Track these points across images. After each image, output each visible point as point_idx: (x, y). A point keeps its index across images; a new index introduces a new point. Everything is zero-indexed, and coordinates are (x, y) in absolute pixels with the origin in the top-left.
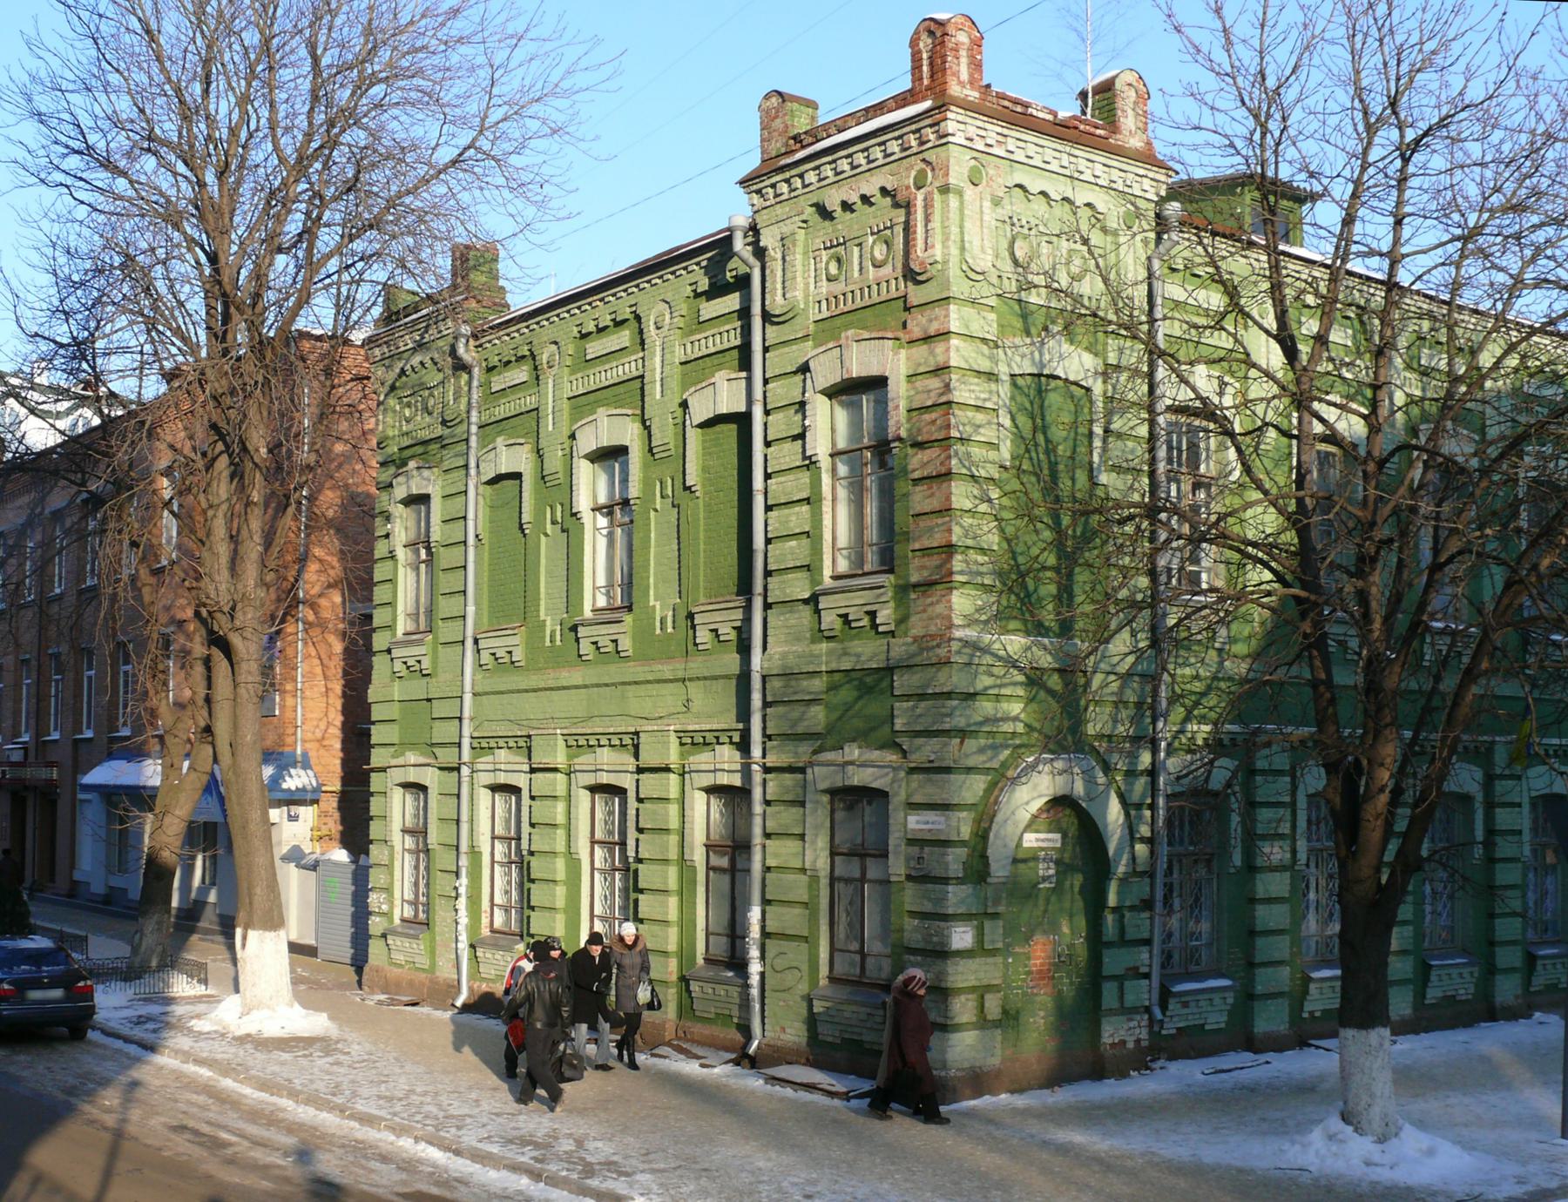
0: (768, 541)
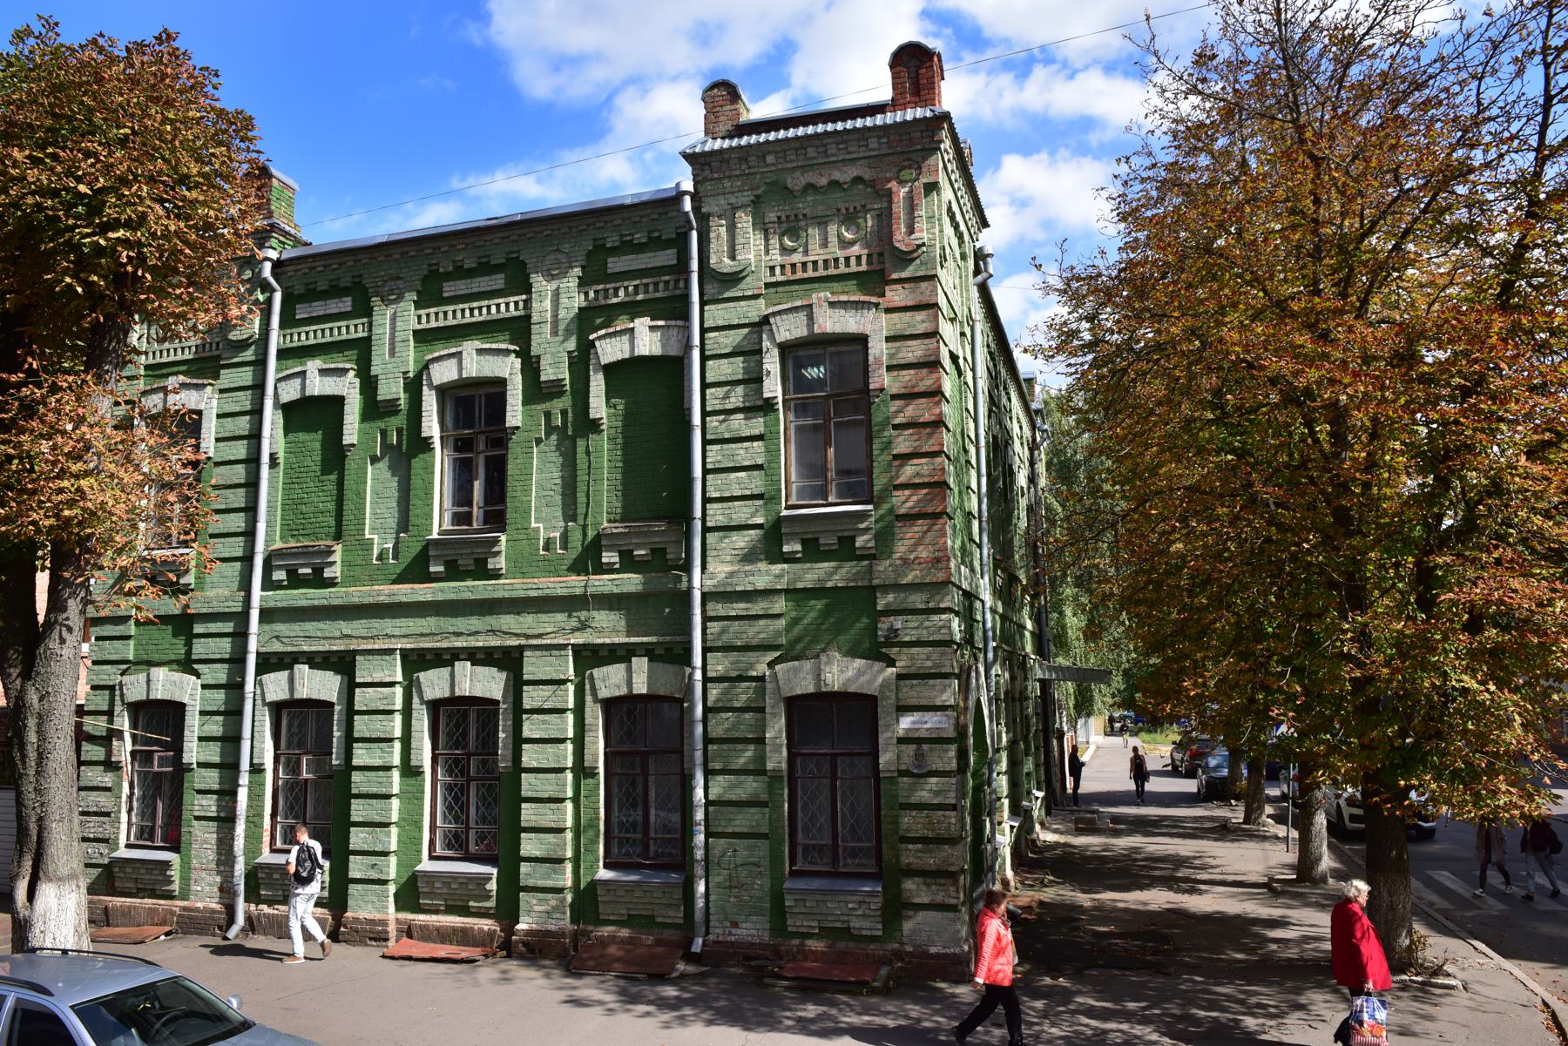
0: (706, 472)
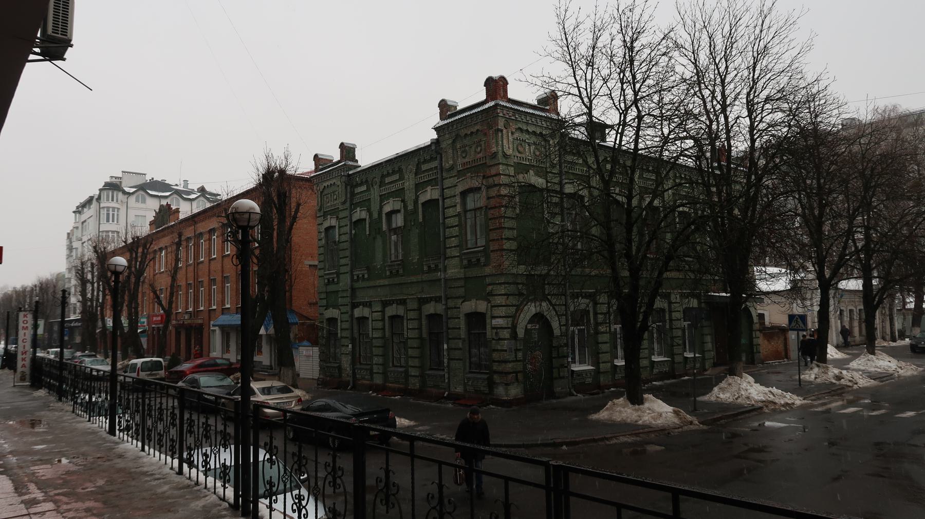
0: (445, 238)
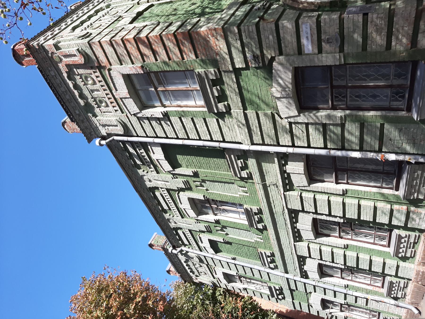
0: (200, 139)
